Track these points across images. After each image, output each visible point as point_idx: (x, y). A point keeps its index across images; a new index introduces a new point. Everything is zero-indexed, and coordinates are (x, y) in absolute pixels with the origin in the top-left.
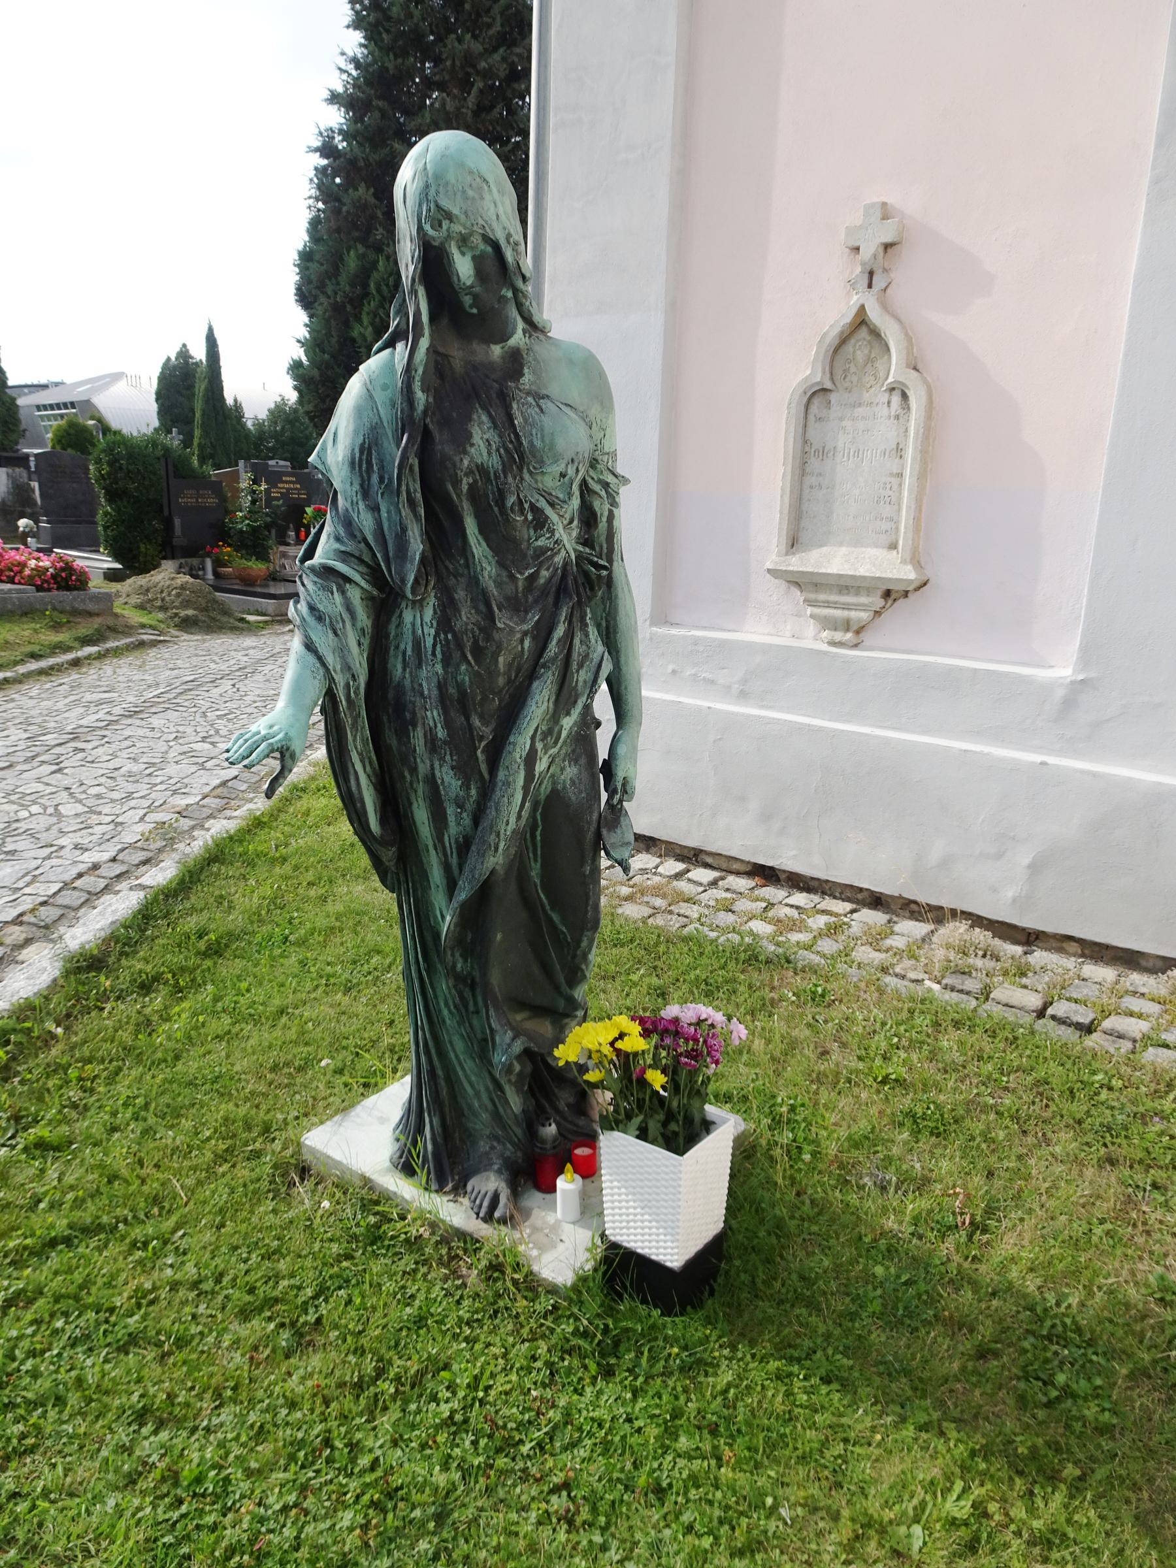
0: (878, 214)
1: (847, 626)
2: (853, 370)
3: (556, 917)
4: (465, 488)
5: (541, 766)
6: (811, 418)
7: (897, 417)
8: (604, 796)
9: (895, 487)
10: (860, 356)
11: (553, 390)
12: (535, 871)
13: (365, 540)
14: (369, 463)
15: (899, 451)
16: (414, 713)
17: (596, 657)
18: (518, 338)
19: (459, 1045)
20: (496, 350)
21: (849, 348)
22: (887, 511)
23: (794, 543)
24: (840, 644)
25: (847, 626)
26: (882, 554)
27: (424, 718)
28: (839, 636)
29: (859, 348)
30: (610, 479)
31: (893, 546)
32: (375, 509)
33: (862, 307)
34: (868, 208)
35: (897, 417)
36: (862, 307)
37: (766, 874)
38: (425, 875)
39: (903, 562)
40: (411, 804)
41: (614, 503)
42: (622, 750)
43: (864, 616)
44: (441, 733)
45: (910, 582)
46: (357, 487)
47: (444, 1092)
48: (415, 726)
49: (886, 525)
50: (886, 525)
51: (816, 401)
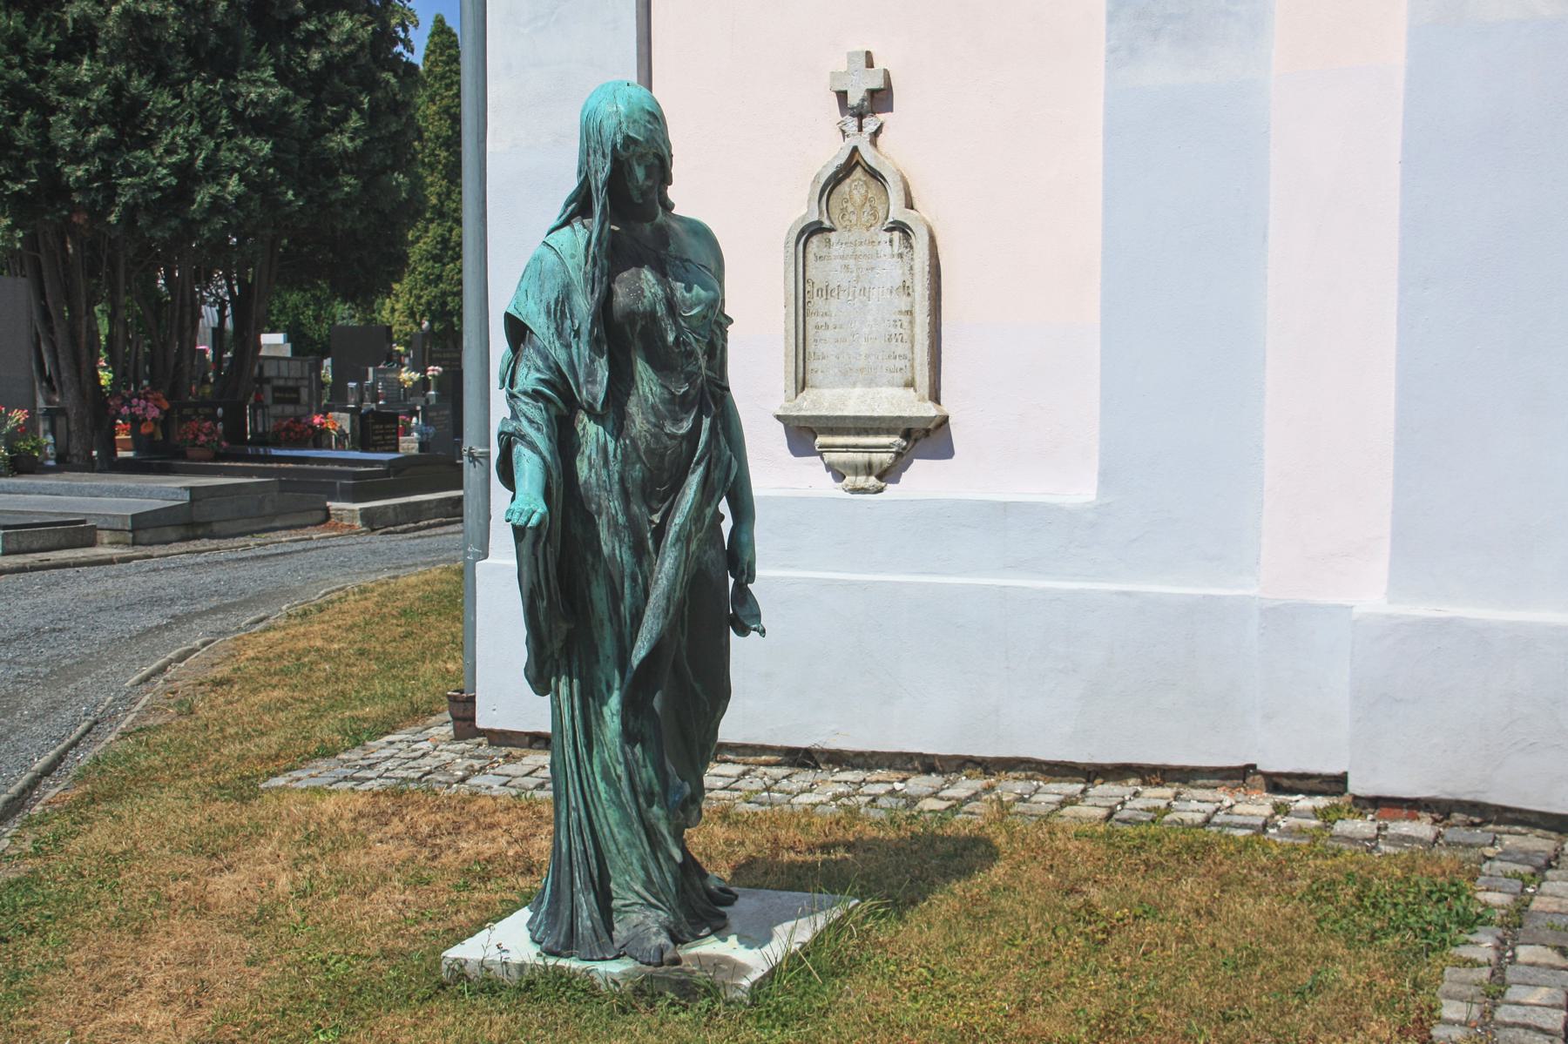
0: (863, 61)
1: (869, 469)
2: (851, 209)
3: (697, 686)
4: (638, 328)
5: (693, 546)
6: (810, 257)
7: (901, 256)
8: (731, 581)
9: (906, 324)
10: (857, 197)
11: (691, 255)
12: (684, 640)
13: (559, 369)
14: (563, 313)
15: (906, 289)
16: (599, 505)
17: (725, 458)
18: (660, 217)
19: (613, 816)
20: (647, 227)
21: (845, 186)
22: (902, 349)
23: (802, 385)
24: (864, 491)
25: (869, 469)
26: (901, 392)
27: (608, 508)
28: (861, 481)
29: (855, 186)
30: (723, 320)
31: (910, 384)
32: (568, 346)
33: (855, 149)
34: (851, 56)
35: (901, 256)
36: (855, 149)
37: (801, 758)
38: (593, 650)
39: (922, 399)
40: (589, 584)
41: (725, 340)
42: (744, 538)
43: (886, 458)
44: (621, 519)
45: (931, 419)
46: (552, 330)
47: (595, 873)
48: (600, 515)
49: (900, 363)
50: (900, 363)
51: (815, 240)
